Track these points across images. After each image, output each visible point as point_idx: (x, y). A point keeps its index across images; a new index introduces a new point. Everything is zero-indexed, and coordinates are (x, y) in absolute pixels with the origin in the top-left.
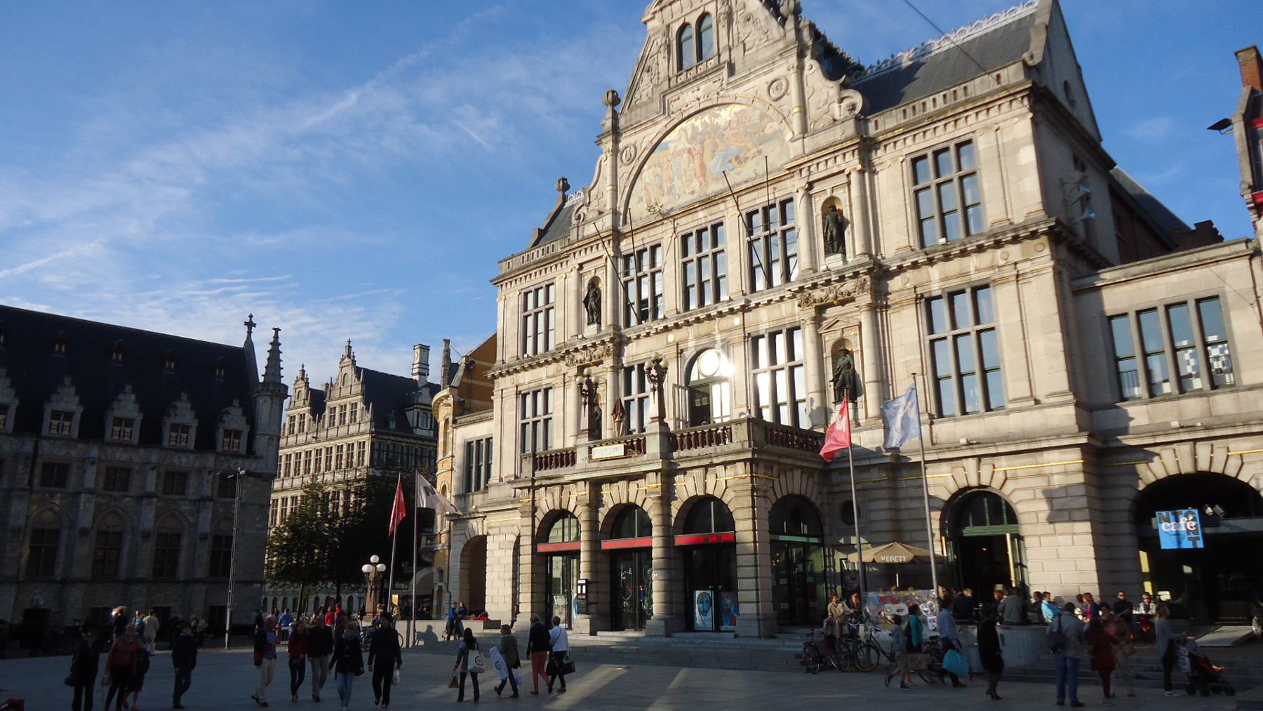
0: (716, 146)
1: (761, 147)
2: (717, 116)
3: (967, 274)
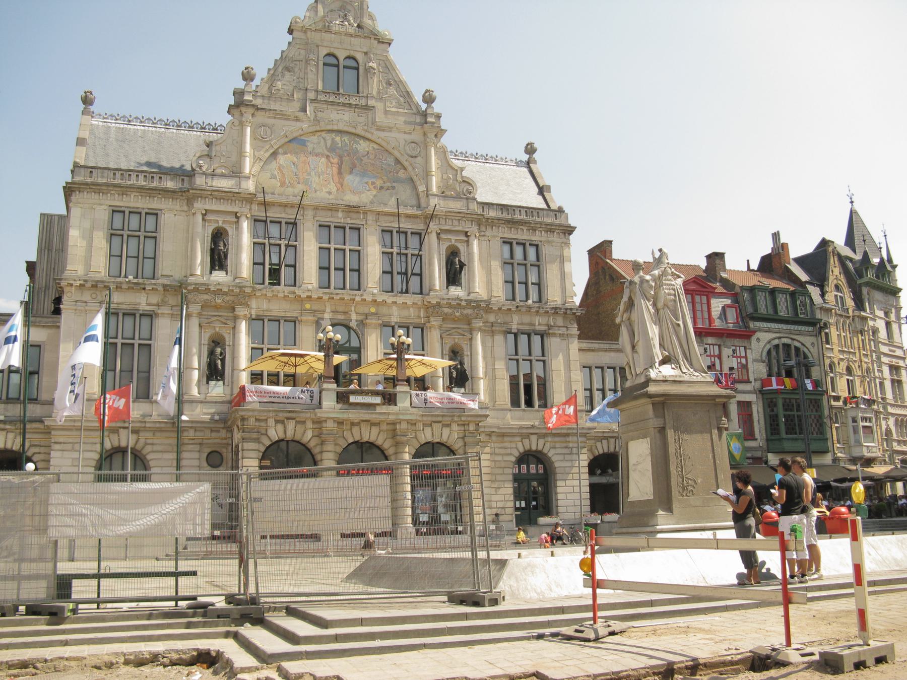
0: (354, 166)
1: (394, 184)
2: (358, 143)
3: (534, 325)
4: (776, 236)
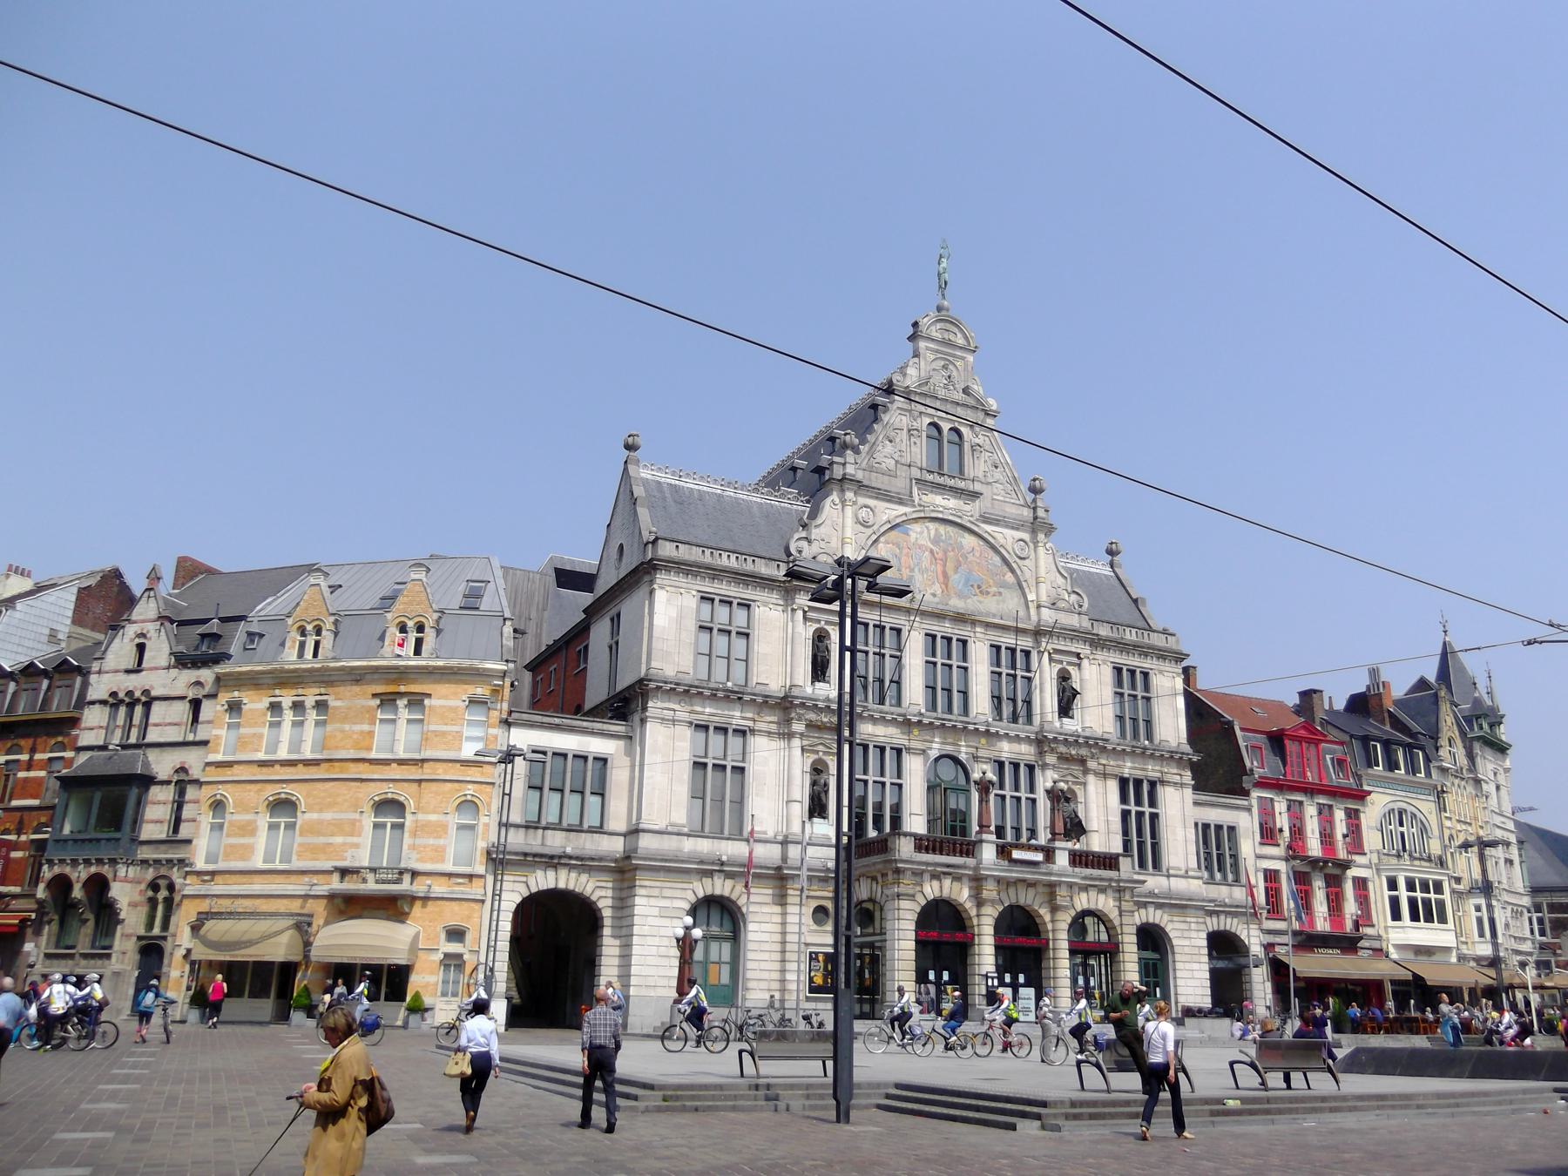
1: (1002, 590)
4: (1374, 673)
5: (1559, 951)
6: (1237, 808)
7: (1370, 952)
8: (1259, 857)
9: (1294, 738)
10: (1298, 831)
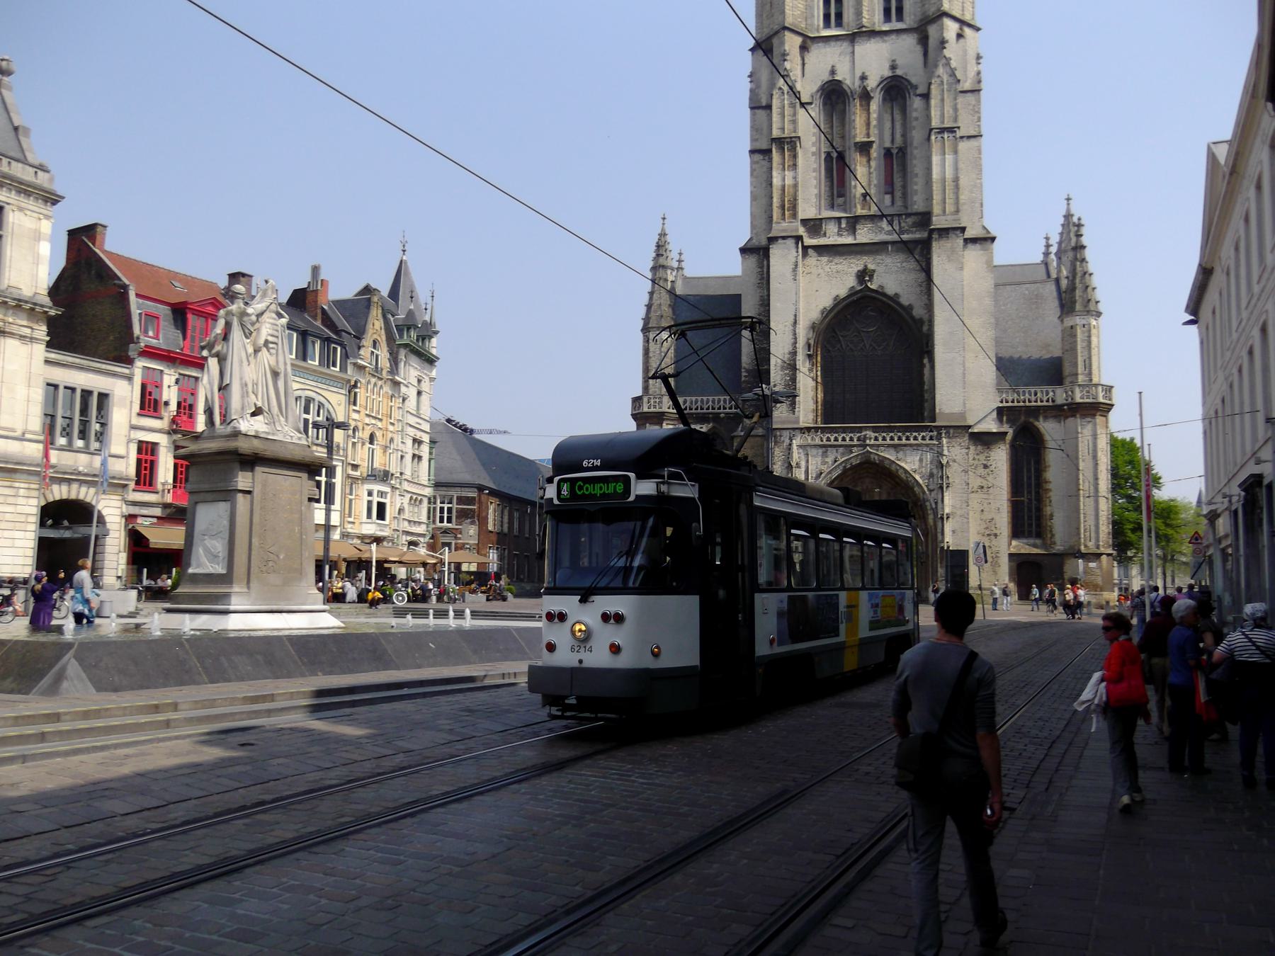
4: (315, 270)
5: (459, 536)
6: (114, 375)
7: (155, 520)
8: (134, 427)
9: (199, 314)
10: (186, 408)
